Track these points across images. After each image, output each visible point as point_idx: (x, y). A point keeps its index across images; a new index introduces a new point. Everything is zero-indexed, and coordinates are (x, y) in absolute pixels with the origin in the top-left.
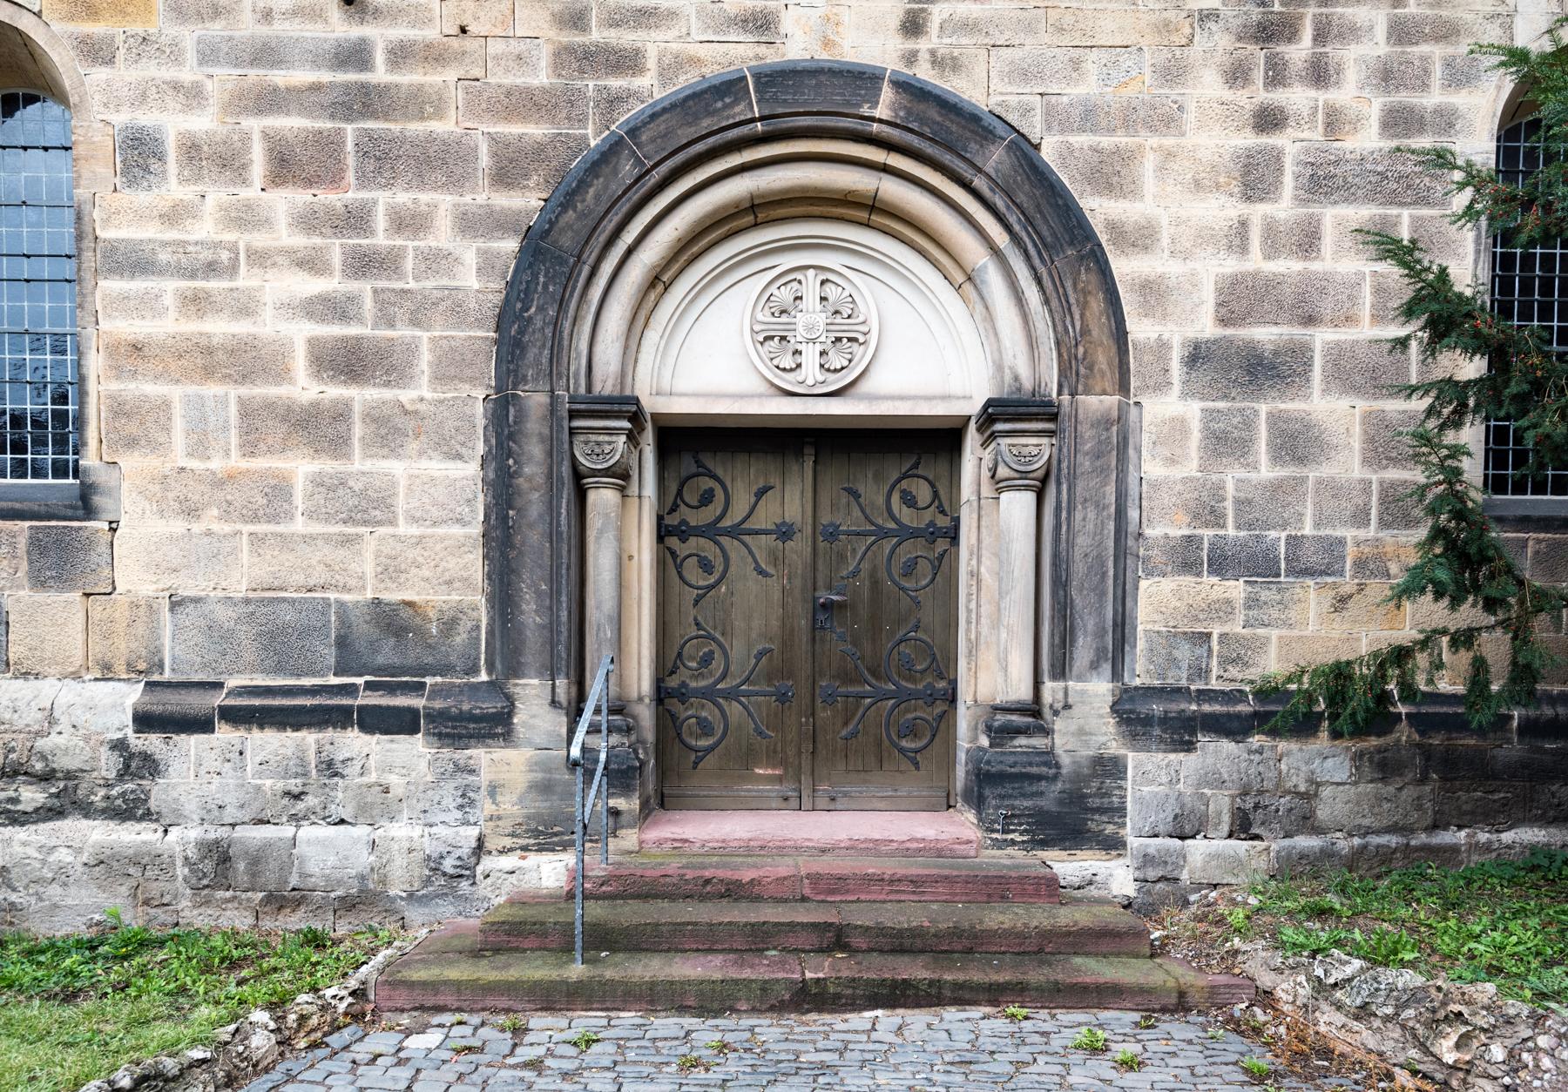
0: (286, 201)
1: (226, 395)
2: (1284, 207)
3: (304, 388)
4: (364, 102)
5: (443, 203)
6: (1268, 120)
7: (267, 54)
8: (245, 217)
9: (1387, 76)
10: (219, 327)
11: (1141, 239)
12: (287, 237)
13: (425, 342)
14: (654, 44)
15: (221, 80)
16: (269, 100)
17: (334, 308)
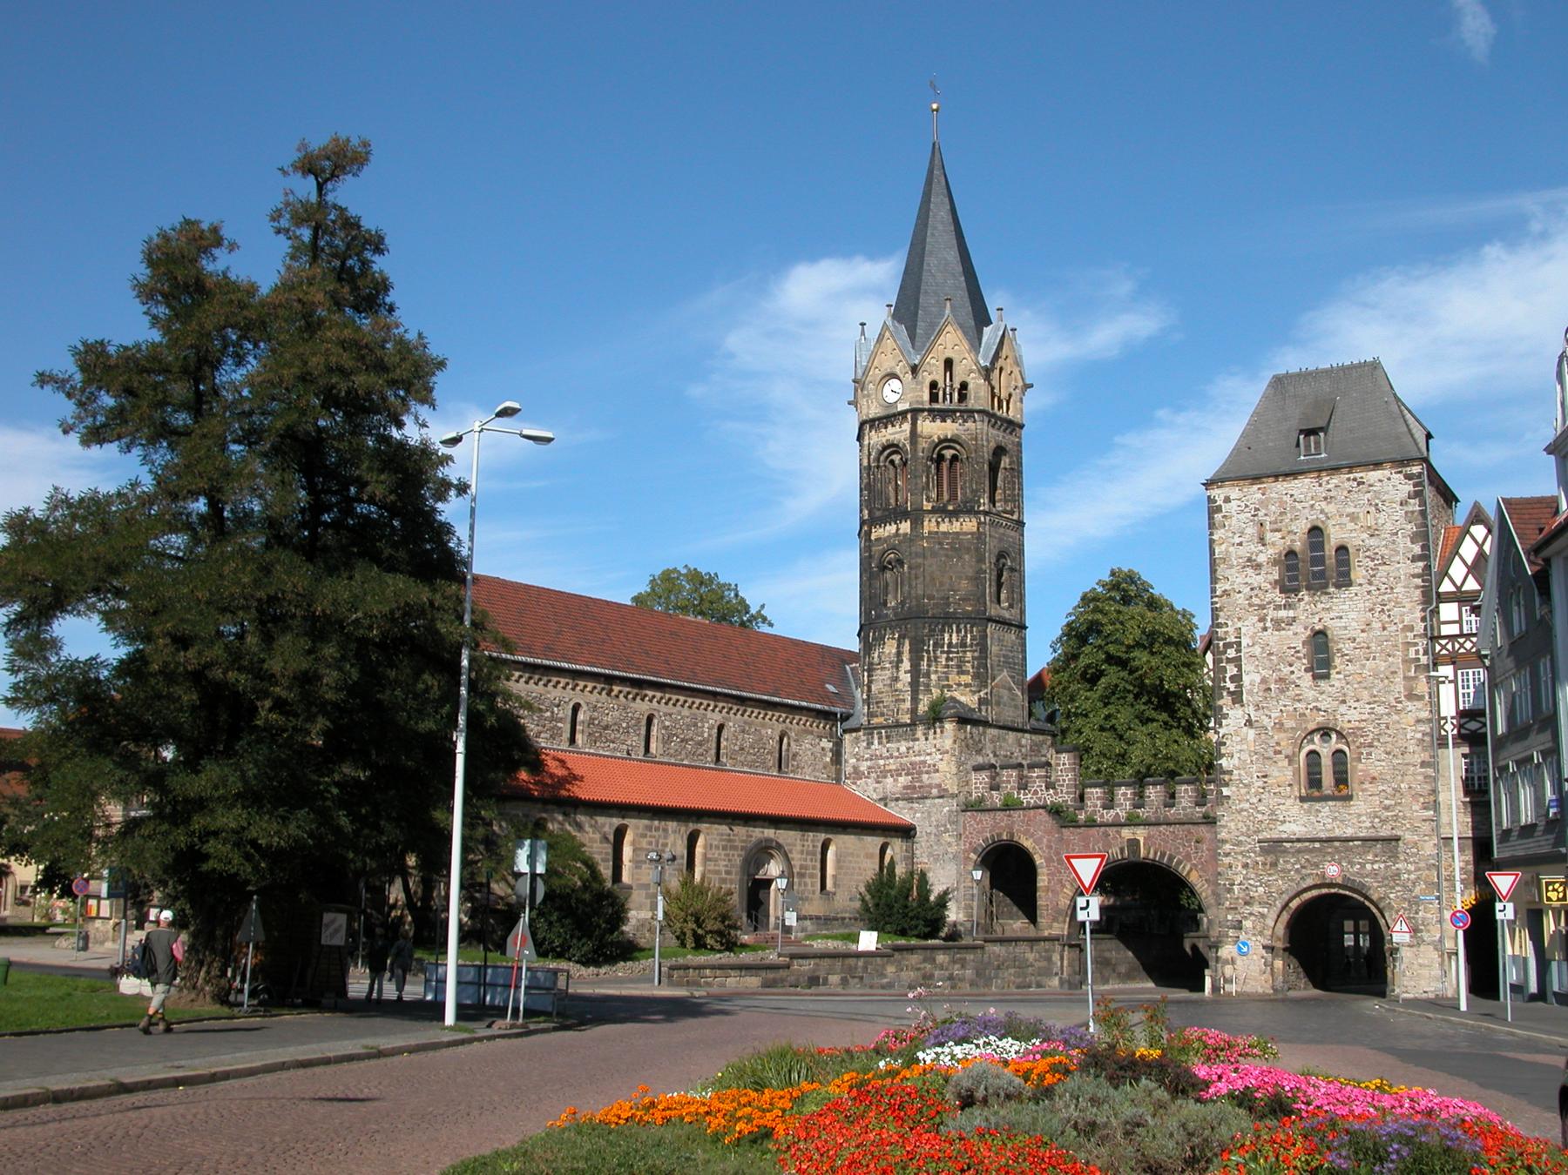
0: (723, 853)
1: (717, 876)
2: (804, 856)
3: (724, 876)
4: (730, 841)
5: (736, 853)
6: (803, 846)
7: (722, 835)
8: (719, 854)
9: (812, 841)
10: (717, 868)
11: (793, 859)
12: (723, 857)
13: (734, 870)
14: (754, 834)
15: (718, 838)
16: (721, 840)
17: (726, 866)
